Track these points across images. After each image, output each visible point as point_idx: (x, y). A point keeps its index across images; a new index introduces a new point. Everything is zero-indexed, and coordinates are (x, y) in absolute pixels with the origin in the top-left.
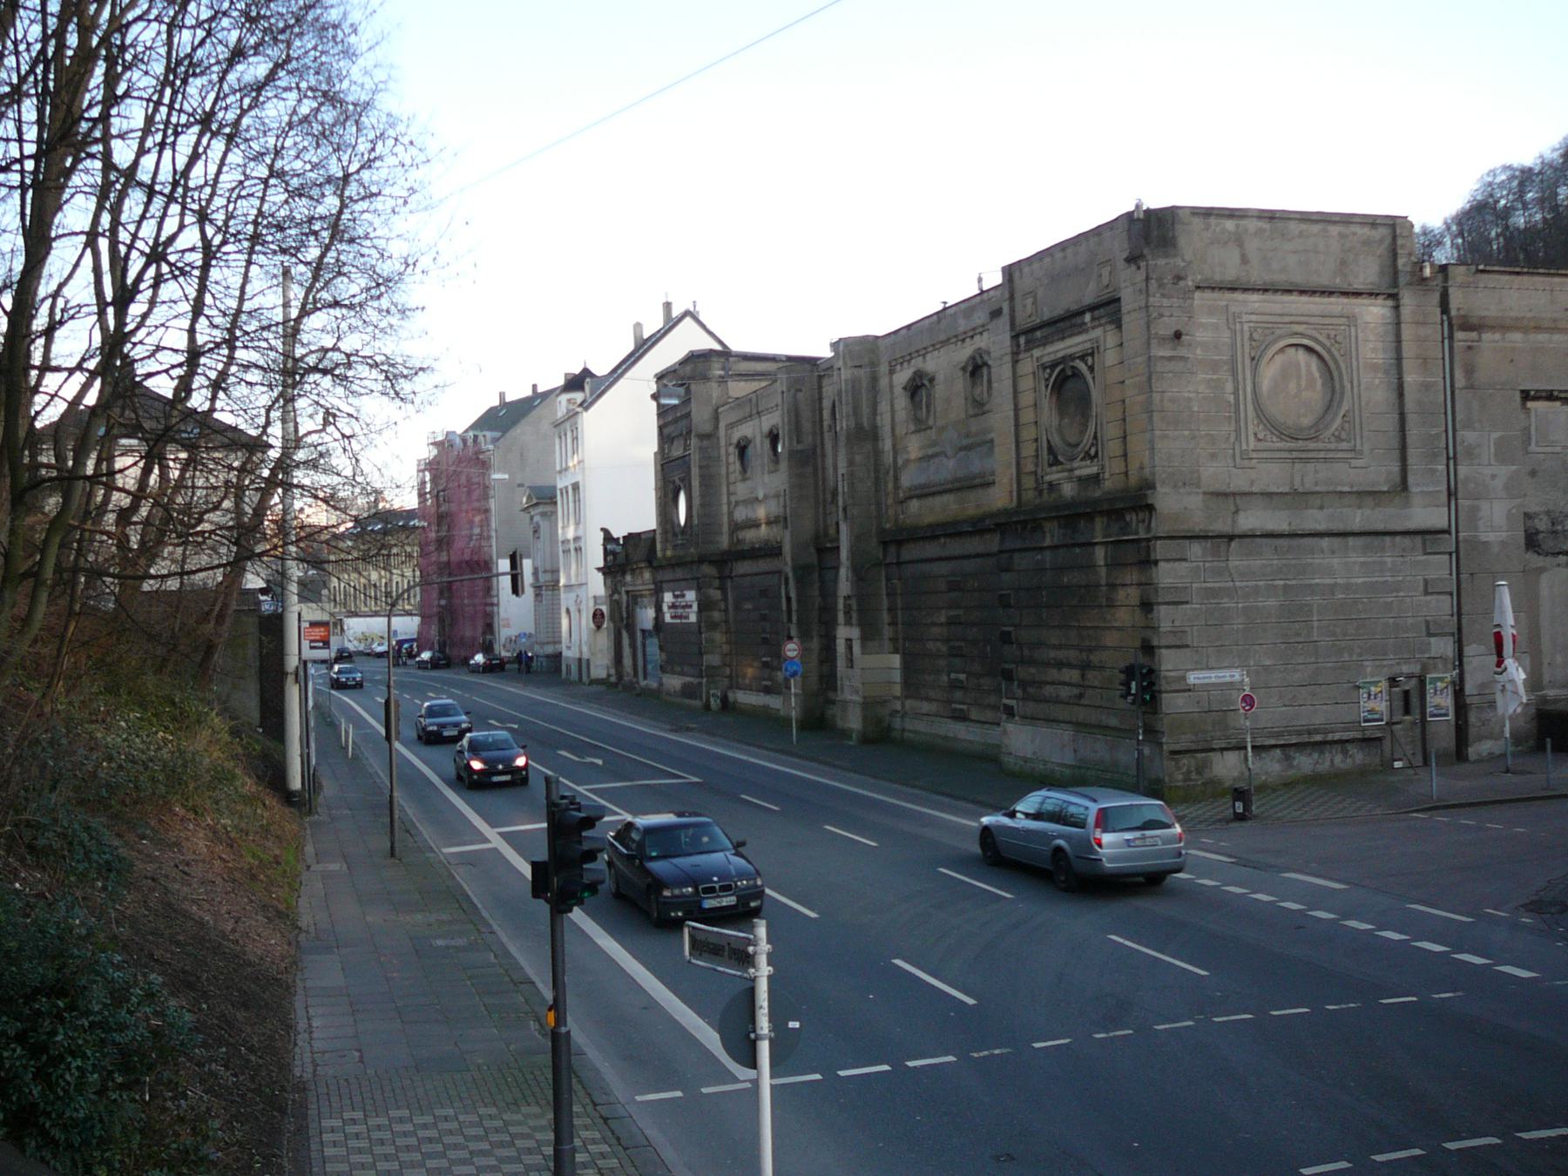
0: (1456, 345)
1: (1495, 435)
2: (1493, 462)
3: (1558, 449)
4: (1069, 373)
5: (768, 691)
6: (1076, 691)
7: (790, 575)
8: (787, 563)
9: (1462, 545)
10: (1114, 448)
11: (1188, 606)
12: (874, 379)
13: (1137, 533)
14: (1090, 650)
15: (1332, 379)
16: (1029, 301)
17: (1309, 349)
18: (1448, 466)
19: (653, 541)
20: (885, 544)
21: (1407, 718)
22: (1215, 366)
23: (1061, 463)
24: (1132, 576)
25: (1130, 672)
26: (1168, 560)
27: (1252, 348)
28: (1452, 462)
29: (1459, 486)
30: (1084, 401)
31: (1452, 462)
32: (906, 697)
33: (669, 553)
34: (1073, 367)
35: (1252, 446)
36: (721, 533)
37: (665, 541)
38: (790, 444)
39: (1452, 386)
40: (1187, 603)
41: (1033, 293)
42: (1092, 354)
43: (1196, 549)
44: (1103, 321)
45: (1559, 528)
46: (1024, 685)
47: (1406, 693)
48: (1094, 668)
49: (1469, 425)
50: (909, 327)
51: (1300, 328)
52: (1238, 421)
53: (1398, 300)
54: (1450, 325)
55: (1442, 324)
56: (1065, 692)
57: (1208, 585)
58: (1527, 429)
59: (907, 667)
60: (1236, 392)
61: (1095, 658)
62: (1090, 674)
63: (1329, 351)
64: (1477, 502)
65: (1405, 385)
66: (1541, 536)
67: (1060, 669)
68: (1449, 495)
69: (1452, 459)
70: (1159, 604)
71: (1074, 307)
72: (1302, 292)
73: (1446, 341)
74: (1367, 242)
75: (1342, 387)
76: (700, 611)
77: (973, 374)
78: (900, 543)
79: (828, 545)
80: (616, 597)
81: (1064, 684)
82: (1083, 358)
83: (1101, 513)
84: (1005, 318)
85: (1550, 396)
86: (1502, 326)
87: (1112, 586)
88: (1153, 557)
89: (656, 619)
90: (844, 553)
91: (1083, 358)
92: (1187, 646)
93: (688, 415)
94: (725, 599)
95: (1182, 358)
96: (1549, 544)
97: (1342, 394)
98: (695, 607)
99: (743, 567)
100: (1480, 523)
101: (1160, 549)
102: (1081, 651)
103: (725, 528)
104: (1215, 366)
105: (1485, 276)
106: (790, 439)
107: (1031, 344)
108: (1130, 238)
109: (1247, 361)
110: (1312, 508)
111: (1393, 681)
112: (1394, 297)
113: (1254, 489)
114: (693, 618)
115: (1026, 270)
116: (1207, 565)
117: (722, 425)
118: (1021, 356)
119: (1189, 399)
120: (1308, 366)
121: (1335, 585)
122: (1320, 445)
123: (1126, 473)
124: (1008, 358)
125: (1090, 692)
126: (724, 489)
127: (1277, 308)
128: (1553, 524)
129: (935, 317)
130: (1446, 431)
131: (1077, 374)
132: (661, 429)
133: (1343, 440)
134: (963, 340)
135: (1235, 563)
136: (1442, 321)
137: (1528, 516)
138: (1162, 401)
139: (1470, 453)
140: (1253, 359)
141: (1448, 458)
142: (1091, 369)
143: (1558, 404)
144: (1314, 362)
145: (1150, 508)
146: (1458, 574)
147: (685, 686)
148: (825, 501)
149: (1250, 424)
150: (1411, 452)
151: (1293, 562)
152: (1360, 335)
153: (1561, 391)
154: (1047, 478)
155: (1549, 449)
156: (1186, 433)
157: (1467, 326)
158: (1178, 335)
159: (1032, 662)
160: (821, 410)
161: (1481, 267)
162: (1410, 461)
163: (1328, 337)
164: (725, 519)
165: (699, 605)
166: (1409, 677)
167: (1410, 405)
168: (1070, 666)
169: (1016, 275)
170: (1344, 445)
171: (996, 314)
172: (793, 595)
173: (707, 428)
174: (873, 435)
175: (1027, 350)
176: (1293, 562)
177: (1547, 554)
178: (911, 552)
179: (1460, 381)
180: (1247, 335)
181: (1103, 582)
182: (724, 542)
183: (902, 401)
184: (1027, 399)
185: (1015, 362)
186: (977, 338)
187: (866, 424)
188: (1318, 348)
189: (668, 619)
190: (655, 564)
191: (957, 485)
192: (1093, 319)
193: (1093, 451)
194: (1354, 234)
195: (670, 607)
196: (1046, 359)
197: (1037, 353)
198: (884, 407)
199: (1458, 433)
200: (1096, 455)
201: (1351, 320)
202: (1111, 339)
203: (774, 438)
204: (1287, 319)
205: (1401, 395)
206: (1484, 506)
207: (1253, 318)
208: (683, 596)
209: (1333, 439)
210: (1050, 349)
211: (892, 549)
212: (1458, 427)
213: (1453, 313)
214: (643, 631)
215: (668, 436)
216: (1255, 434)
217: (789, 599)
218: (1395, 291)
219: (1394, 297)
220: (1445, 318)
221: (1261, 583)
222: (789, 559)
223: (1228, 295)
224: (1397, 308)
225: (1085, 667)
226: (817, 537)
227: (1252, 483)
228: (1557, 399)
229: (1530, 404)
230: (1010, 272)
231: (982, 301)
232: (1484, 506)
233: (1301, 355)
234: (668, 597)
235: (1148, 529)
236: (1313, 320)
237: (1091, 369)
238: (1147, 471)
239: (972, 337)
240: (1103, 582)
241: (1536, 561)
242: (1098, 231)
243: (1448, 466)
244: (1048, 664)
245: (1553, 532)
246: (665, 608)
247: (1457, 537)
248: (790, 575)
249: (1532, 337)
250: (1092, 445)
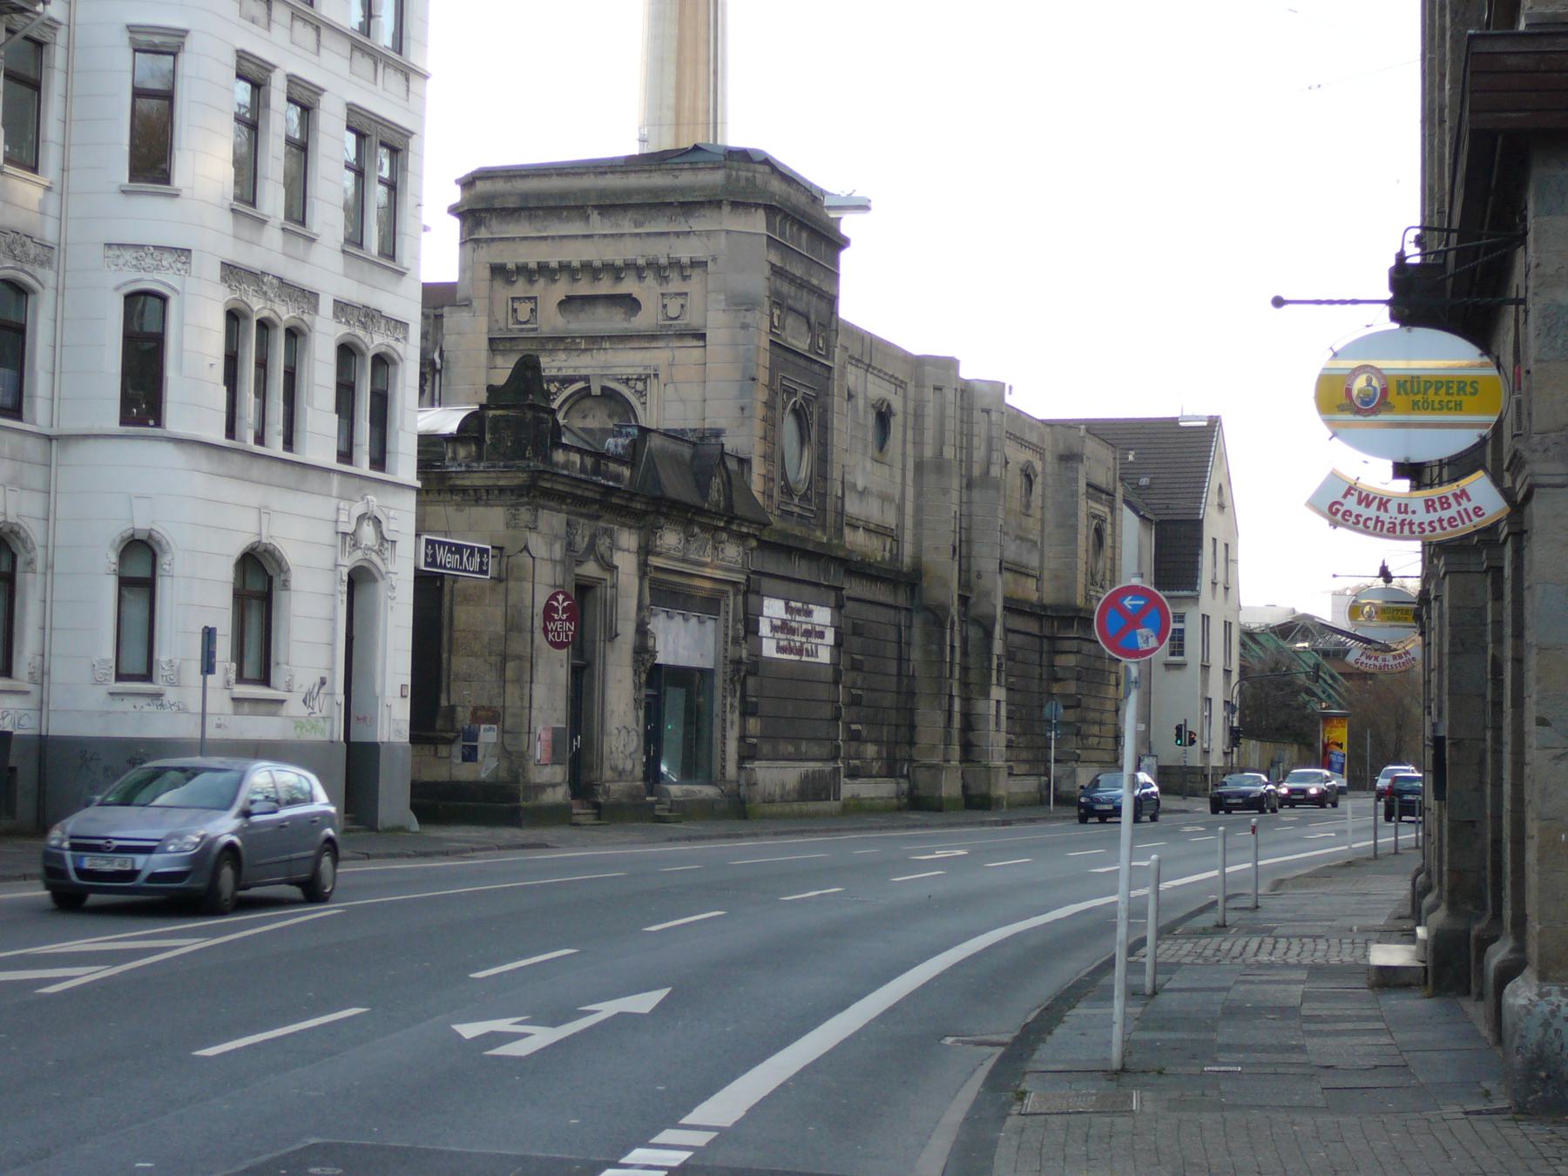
7: (956, 618)
76: (838, 645)
80: (590, 569)
98: (830, 637)
114: (824, 656)
147: (806, 779)
172: (957, 644)
189: (769, 649)
191: (1014, 567)
195: (774, 628)
208: (809, 613)
234: (774, 608)
246: (764, 628)
248: (956, 618)
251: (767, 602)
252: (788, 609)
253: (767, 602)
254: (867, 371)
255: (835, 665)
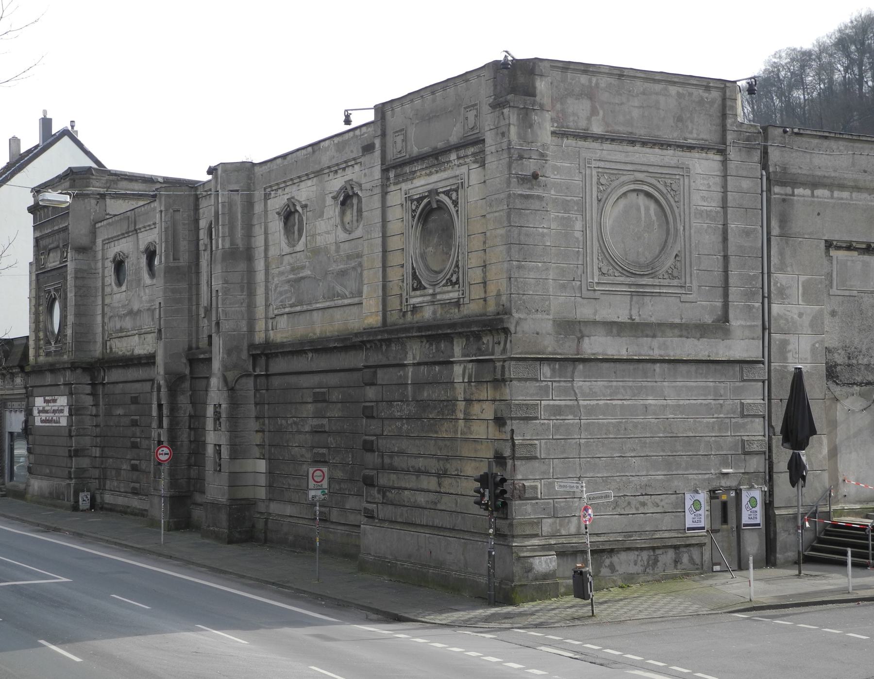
0: (773, 196)
1: (802, 278)
2: (800, 302)
3: (855, 293)
4: (435, 206)
5: (135, 492)
6: (432, 497)
7: (162, 382)
8: (159, 371)
9: (773, 374)
10: (476, 275)
11: (538, 421)
12: (249, 204)
13: (493, 354)
14: (447, 459)
15: (667, 222)
16: (399, 139)
17: (648, 195)
18: (763, 303)
19: (26, 347)
20: (255, 358)
21: (725, 527)
22: (565, 206)
23: (425, 288)
24: (486, 392)
25: (484, 480)
26: (520, 380)
27: (599, 191)
28: (766, 300)
29: (772, 322)
30: (447, 231)
31: (766, 300)
32: (270, 500)
33: (42, 359)
34: (438, 201)
35: (596, 280)
36: (95, 342)
37: (37, 348)
38: (166, 262)
39: (769, 233)
40: (536, 418)
41: (402, 131)
42: (456, 190)
43: (546, 370)
44: (467, 160)
45: (854, 361)
46: (383, 490)
47: (724, 505)
48: (451, 476)
49: (782, 269)
50: (284, 157)
51: (640, 176)
52: (585, 255)
53: (726, 155)
54: (768, 179)
55: (761, 179)
56: (421, 499)
57: (557, 403)
58: (830, 275)
59: (270, 472)
60: (584, 231)
61: (452, 467)
62: (446, 482)
63: (666, 199)
64: (787, 337)
65: (729, 231)
66: (839, 368)
67: (417, 477)
68: (764, 329)
69: (766, 298)
70: (512, 419)
71: (440, 145)
72: (644, 144)
73: (765, 194)
74: (701, 102)
75: (676, 230)
77: (343, 203)
78: (268, 356)
79: (202, 356)
81: (422, 490)
82: (447, 193)
83: (460, 334)
84: (377, 153)
85: (849, 248)
86: (814, 184)
87: (469, 401)
88: (507, 376)
89: (26, 422)
90: (216, 365)
91: (447, 193)
92: (536, 458)
93: (65, 229)
94: (96, 405)
95: (540, 198)
96: (845, 376)
97: (676, 235)
98: (66, 413)
99: (115, 375)
100: (790, 355)
101: (513, 370)
102: (439, 459)
103: (99, 339)
104: (565, 206)
105: (798, 139)
106: (167, 257)
107: (401, 178)
108: (495, 86)
109: (595, 202)
110: (647, 336)
111: (713, 494)
112: (722, 152)
113: (598, 318)
114: (64, 422)
115: (398, 110)
116: (554, 384)
117: (99, 242)
118: (392, 188)
119: (543, 235)
120: (647, 209)
121: (666, 406)
122: (656, 282)
123: (485, 300)
124: (378, 190)
125: (446, 499)
126: (100, 302)
127: (620, 157)
128: (849, 358)
129: (310, 149)
130: (763, 273)
131: (441, 207)
132: (37, 240)
133: (675, 278)
134: (336, 172)
135: (579, 383)
136: (762, 175)
137: (828, 350)
138: (519, 234)
139: (782, 293)
140: (599, 201)
141: (763, 297)
142: (455, 203)
143: (855, 253)
144: (653, 206)
145: (506, 331)
146: (769, 400)
148: (198, 315)
149: (595, 260)
150: (732, 290)
151: (630, 384)
152: (692, 184)
153: (857, 242)
154: (413, 301)
155: (847, 293)
156: (540, 264)
157: (783, 184)
158: (535, 176)
159: (393, 469)
160: (197, 229)
161: (796, 130)
162: (731, 298)
163: (666, 185)
164: (99, 330)
165: (70, 410)
166: (728, 489)
167: (732, 250)
168: (427, 473)
169: (389, 114)
170: (675, 282)
171: (368, 148)
173: (85, 241)
174: (248, 255)
175: (395, 184)
176: (630, 384)
177: (844, 384)
178: (279, 365)
179: (775, 231)
180: (595, 180)
181: (461, 397)
182: (97, 351)
183: (276, 226)
184: (395, 227)
185: (384, 194)
186: (349, 171)
187: (240, 245)
188: (656, 194)
189: (38, 422)
190: (28, 369)
192: (459, 158)
193: (454, 279)
194: (690, 94)
195: (39, 412)
196: (412, 192)
197: (405, 186)
198: (258, 231)
199: (773, 276)
200: (457, 282)
201: (685, 170)
202: (475, 175)
203: (151, 255)
204: (629, 167)
205: (725, 239)
206: (792, 339)
207: (602, 164)
209: (666, 276)
210: (418, 182)
211: (262, 361)
212: (772, 270)
213: (771, 169)
214: (11, 434)
215: (45, 248)
216: (600, 269)
217: (160, 406)
218: (722, 147)
219: (722, 152)
220: (764, 173)
221: (601, 402)
222: (161, 370)
223: (581, 143)
224: (724, 162)
225: (442, 475)
226: (190, 348)
227: (595, 314)
228: (856, 249)
229: (833, 253)
230: (381, 110)
231: (355, 136)
232: (792, 339)
233: (642, 200)
234: (39, 402)
235: (504, 350)
236: (651, 169)
237: (455, 203)
238: (504, 298)
239: (344, 169)
240: (461, 397)
241: (838, 390)
242: (465, 77)
243: (763, 303)
244: (407, 471)
245: (849, 365)
246: (35, 412)
247: (769, 366)
248: (162, 382)
249: (836, 194)
250: (454, 272)
251: (37, 399)
252: (46, 401)
253: (37, 399)
254: (137, 233)
255: (70, 425)
